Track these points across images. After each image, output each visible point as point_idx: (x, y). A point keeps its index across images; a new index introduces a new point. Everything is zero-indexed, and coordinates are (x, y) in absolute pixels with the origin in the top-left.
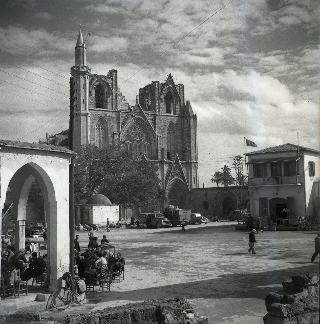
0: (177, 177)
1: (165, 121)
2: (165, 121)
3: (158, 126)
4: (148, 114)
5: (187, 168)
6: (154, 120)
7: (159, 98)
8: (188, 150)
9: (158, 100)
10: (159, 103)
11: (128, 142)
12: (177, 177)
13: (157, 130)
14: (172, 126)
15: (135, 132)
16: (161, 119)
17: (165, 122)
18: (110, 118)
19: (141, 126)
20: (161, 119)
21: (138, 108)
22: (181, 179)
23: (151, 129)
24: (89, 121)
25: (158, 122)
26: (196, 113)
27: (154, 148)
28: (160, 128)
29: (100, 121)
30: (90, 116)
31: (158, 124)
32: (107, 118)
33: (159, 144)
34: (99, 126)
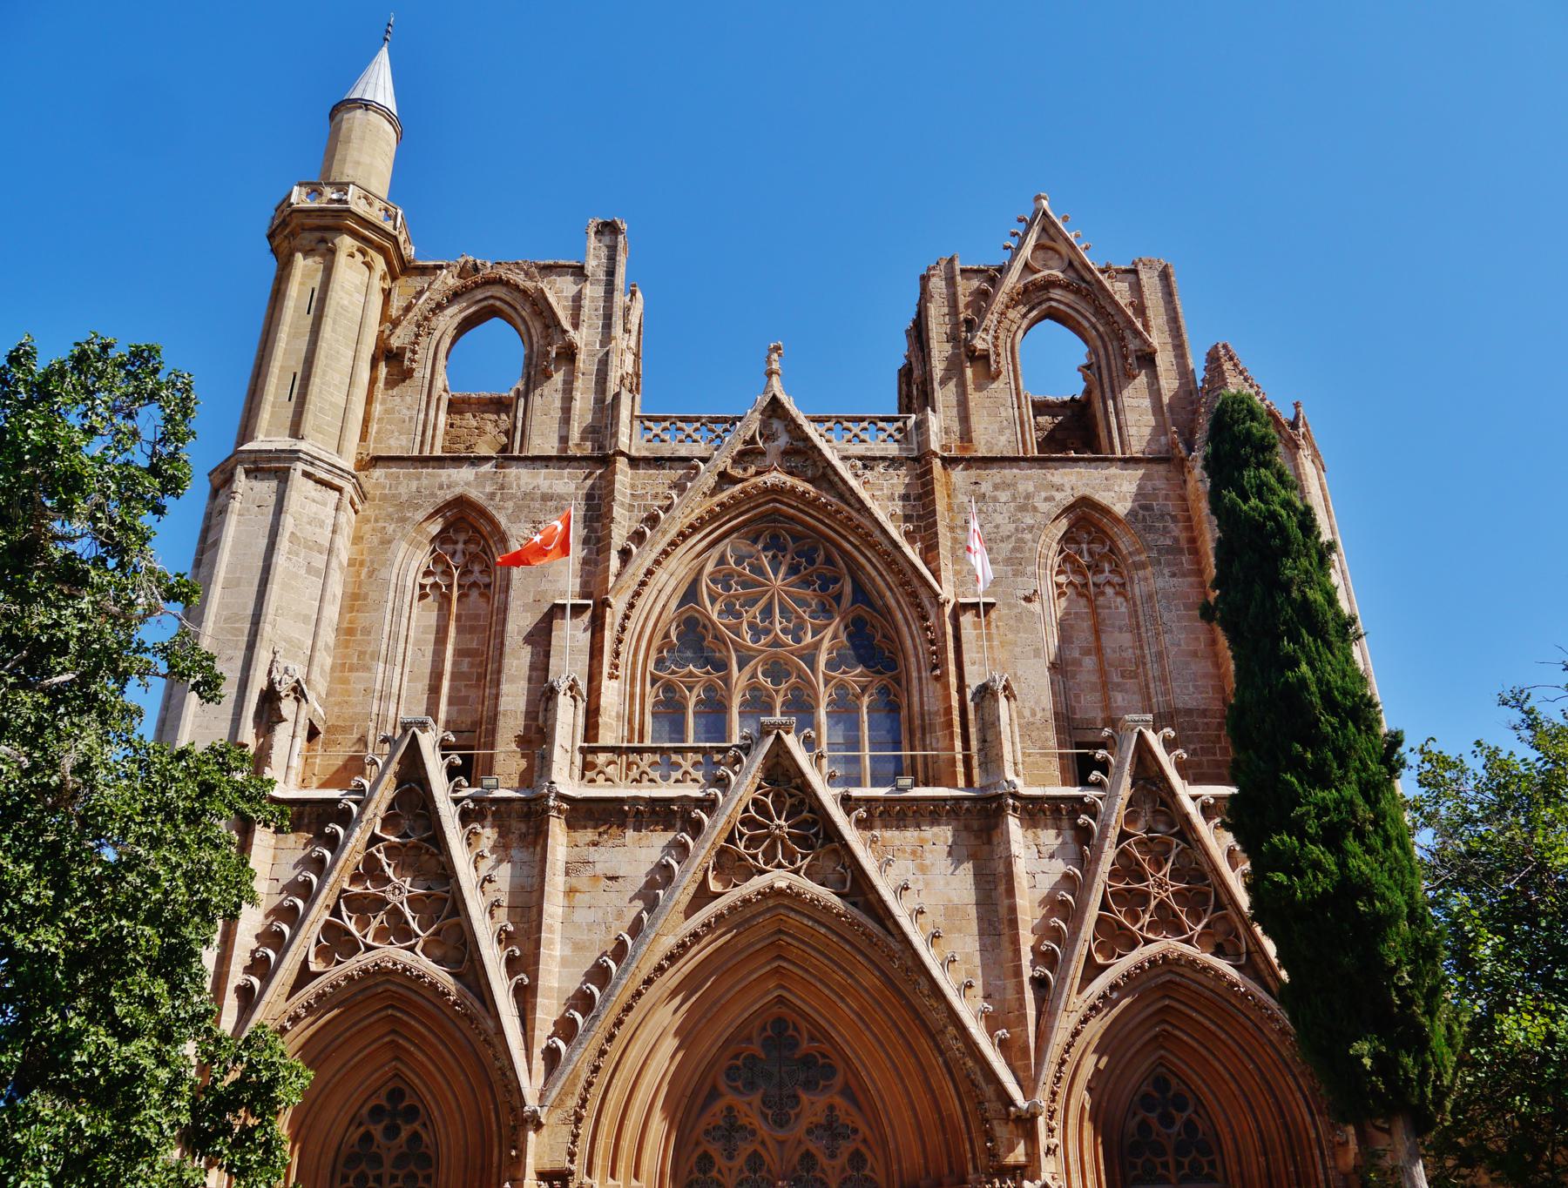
1: (1028, 496)
4: (868, 462)
6: (919, 497)
9: (954, 369)
10: (962, 385)
11: (691, 674)
14: (1101, 535)
16: (986, 487)
17: (1022, 508)
19: (816, 550)
20: (986, 487)
21: (777, 425)
22: (1223, 965)
23: (891, 557)
25: (963, 509)
27: (933, 704)
29: (462, 537)
32: (510, 504)
33: (967, 668)
34: (447, 573)
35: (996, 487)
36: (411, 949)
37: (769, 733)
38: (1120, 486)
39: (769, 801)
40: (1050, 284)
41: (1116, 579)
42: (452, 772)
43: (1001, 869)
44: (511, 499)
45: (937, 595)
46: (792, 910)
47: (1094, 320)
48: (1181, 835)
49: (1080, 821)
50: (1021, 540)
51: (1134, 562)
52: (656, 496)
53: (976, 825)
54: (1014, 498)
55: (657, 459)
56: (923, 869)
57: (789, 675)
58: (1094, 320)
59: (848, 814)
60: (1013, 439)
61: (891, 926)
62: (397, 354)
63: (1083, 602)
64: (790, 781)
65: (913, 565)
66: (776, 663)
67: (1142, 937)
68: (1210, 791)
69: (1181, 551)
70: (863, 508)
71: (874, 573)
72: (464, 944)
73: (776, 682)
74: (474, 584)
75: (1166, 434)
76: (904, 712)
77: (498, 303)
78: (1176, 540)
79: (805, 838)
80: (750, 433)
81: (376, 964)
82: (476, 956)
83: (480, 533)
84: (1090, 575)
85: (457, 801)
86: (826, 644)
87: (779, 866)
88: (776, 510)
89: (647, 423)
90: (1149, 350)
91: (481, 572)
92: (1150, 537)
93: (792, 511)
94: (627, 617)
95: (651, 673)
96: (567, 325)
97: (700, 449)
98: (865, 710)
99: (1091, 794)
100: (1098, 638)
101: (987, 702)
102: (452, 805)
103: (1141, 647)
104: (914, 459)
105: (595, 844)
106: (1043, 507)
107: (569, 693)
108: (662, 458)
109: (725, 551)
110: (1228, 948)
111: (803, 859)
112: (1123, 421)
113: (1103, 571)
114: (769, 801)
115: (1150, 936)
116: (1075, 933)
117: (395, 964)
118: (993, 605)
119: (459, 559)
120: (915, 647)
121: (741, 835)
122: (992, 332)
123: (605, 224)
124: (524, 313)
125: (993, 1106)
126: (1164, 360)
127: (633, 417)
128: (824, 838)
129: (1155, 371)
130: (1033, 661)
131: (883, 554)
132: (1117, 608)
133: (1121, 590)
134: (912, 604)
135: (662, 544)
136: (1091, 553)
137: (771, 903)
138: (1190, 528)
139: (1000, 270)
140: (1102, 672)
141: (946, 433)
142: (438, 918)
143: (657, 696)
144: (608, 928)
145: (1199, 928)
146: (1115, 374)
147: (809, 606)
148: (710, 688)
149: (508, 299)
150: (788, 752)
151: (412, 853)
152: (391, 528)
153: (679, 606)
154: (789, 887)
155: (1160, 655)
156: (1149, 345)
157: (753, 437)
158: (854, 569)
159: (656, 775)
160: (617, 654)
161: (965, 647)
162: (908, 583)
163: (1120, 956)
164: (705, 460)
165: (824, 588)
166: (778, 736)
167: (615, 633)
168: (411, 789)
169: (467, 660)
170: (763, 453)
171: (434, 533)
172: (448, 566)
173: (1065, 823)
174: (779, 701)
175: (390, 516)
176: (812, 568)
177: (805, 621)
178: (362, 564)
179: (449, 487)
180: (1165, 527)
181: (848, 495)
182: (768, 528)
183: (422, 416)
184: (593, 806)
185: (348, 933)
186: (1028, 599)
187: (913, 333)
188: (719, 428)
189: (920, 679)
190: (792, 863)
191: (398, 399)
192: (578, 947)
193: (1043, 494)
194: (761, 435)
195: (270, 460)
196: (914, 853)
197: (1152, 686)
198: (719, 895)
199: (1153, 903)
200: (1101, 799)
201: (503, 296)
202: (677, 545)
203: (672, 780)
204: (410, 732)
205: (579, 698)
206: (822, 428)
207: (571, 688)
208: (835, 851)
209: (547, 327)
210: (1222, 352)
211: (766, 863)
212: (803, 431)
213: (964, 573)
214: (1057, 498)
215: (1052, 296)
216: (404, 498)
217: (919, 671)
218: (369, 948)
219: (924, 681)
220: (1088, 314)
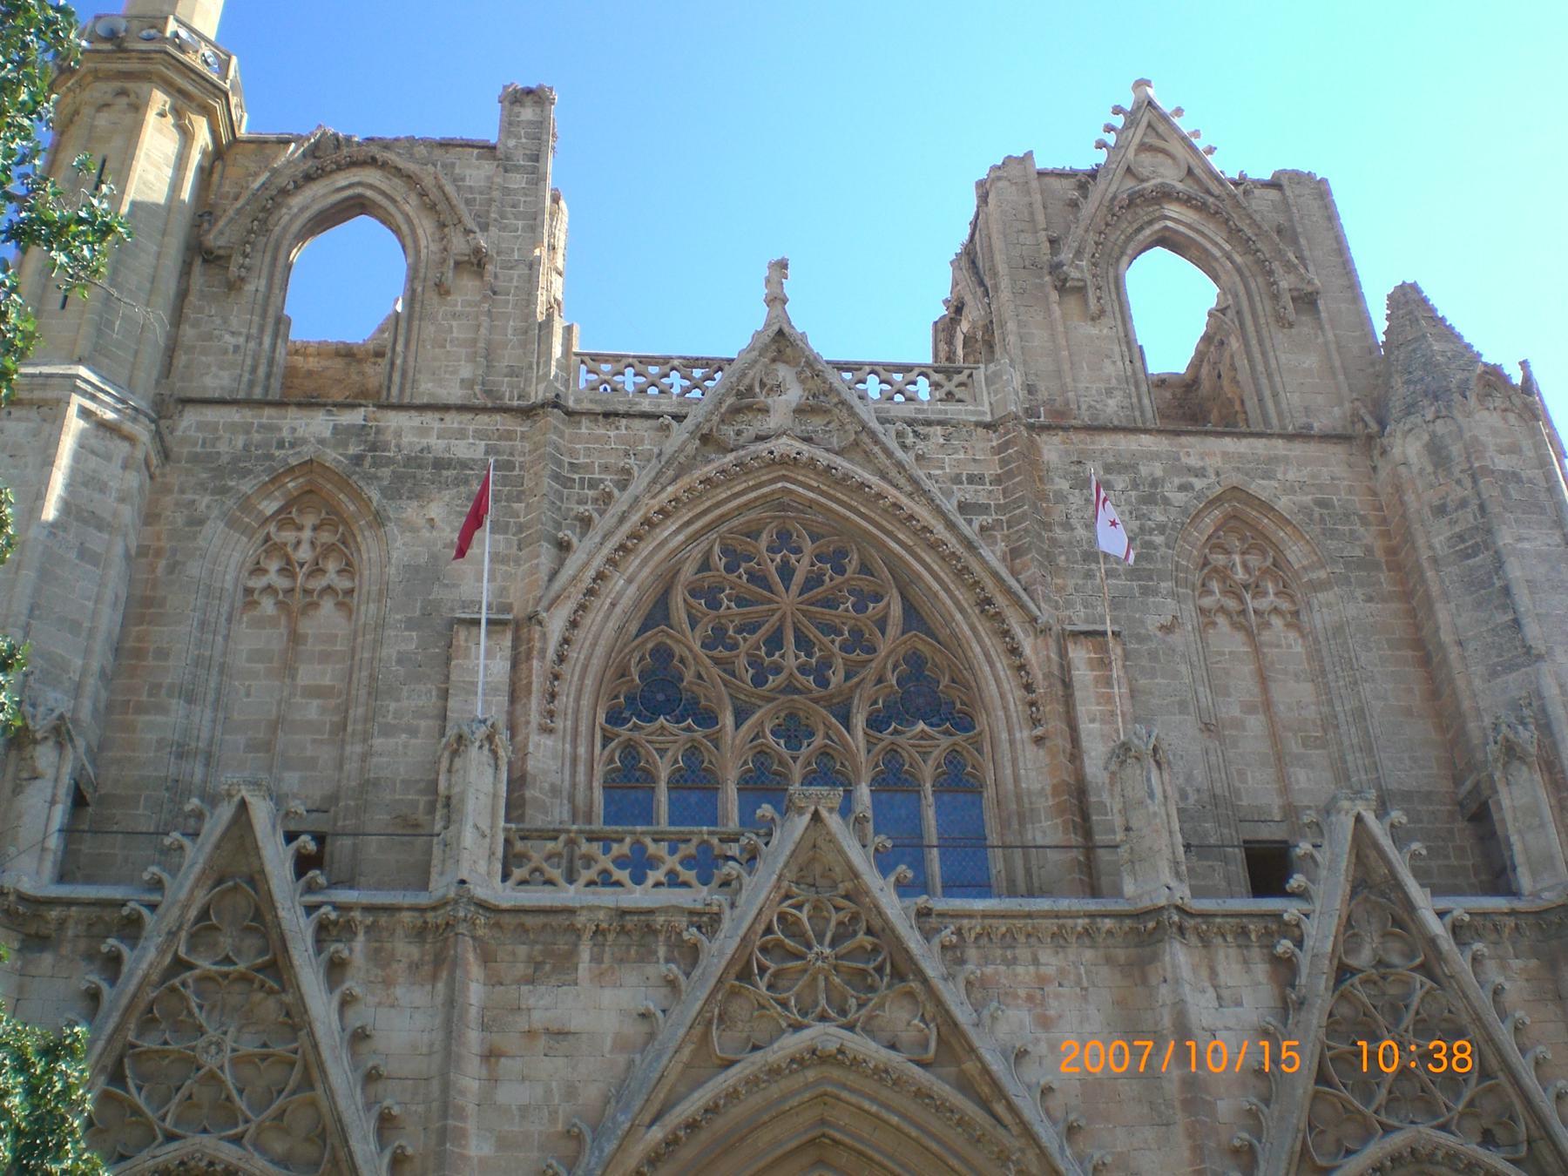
1: (1154, 483)
3: (1058, 532)
6: (998, 480)
8: (1511, 752)
14: (1259, 542)
17: (1149, 500)
18: (427, 473)
19: (842, 553)
21: (784, 372)
26: (1524, 365)
29: (309, 520)
32: (386, 472)
35: (1108, 469)
36: (237, 1140)
37: (801, 811)
38: (1285, 473)
39: (803, 916)
40: (1166, 194)
41: (1285, 605)
42: (304, 864)
43: (1167, 1021)
44: (387, 465)
45: (1035, 619)
46: (844, 1086)
48: (1424, 969)
49: (1280, 949)
50: (1149, 545)
51: (1310, 581)
53: (1121, 954)
54: (1135, 486)
55: (606, 415)
56: (1045, 1023)
57: (812, 734)
58: (1228, 247)
59: (927, 935)
61: (1000, 1108)
62: (219, 257)
63: (1240, 637)
64: (834, 886)
65: (995, 575)
66: (791, 716)
67: (1380, 1123)
68: (1461, 906)
69: (1376, 566)
70: (918, 490)
71: (936, 587)
72: (323, 1135)
73: (793, 740)
74: (329, 589)
75: (1341, 404)
76: (989, 793)
77: (369, 193)
78: (1369, 550)
79: (863, 973)
80: (747, 381)
81: (182, 1163)
82: (342, 1154)
83: (337, 514)
84: (1248, 597)
85: (310, 909)
86: (869, 689)
87: (823, 1018)
88: (784, 489)
90: (1309, 289)
91: (339, 572)
92: (1332, 544)
93: (811, 495)
94: (566, 641)
95: (603, 729)
96: (471, 224)
98: (928, 787)
100: (1265, 690)
101: (1129, 771)
102: (300, 911)
103: (1330, 703)
104: (987, 426)
105: (531, 981)
106: (1179, 498)
107: (487, 746)
108: (617, 415)
109: (712, 547)
110: (1500, 1134)
111: (860, 1006)
112: (1279, 386)
113: (1265, 594)
114: (803, 916)
117: (211, 1164)
119: (304, 554)
120: (1002, 696)
121: (763, 970)
122: (1087, 256)
123: (529, 92)
124: (407, 208)
128: (892, 976)
129: (1319, 319)
130: (1178, 718)
131: (948, 558)
132: (1290, 646)
133: (1294, 620)
134: (995, 633)
136: (1245, 566)
137: (811, 1075)
138: (1386, 534)
139: (1093, 174)
140: (1274, 737)
141: (1030, 392)
142: (280, 1092)
143: (611, 761)
144: (553, 1114)
145: (1460, 1107)
146: (1262, 321)
148: (693, 751)
149: (384, 187)
150: (832, 840)
151: (237, 988)
152: (204, 501)
153: (643, 629)
154: (840, 1051)
155: (1360, 714)
156: (1310, 282)
157: (750, 389)
158: (905, 584)
159: (623, 875)
160: (553, 696)
161: (1078, 694)
162: (989, 601)
163: (1349, 1153)
164: (679, 418)
165: (860, 607)
166: (816, 817)
167: (548, 663)
168: (236, 888)
169: (315, 703)
170: (765, 411)
171: (269, 512)
172: (289, 561)
173: (1256, 953)
174: (797, 771)
175: (202, 487)
176: (839, 579)
177: (833, 654)
178: (158, 553)
179: (292, 445)
180: (1352, 532)
181: (893, 473)
182: (774, 518)
183: (252, 345)
184: (529, 921)
185: (137, 1111)
186: (1167, 629)
187: (964, 263)
188: (697, 373)
189: (1012, 742)
190: (843, 1012)
191: (218, 321)
192: (503, 1143)
193: (1177, 481)
194: (762, 385)
196: (1030, 998)
197: (1350, 758)
198: (731, 1064)
200: (1307, 916)
201: (377, 183)
202: (640, 538)
203: (650, 881)
204: (236, 799)
205: (501, 753)
206: (847, 376)
207: (490, 738)
208: (911, 995)
209: (442, 225)
211: (804, 1014)
213: (1070, 590)
215: (1167, 213)
216: (225, 459)
217: (1010, 731)
218: (171, 1137)
219: (1019, 746)
220: (1221, 242)
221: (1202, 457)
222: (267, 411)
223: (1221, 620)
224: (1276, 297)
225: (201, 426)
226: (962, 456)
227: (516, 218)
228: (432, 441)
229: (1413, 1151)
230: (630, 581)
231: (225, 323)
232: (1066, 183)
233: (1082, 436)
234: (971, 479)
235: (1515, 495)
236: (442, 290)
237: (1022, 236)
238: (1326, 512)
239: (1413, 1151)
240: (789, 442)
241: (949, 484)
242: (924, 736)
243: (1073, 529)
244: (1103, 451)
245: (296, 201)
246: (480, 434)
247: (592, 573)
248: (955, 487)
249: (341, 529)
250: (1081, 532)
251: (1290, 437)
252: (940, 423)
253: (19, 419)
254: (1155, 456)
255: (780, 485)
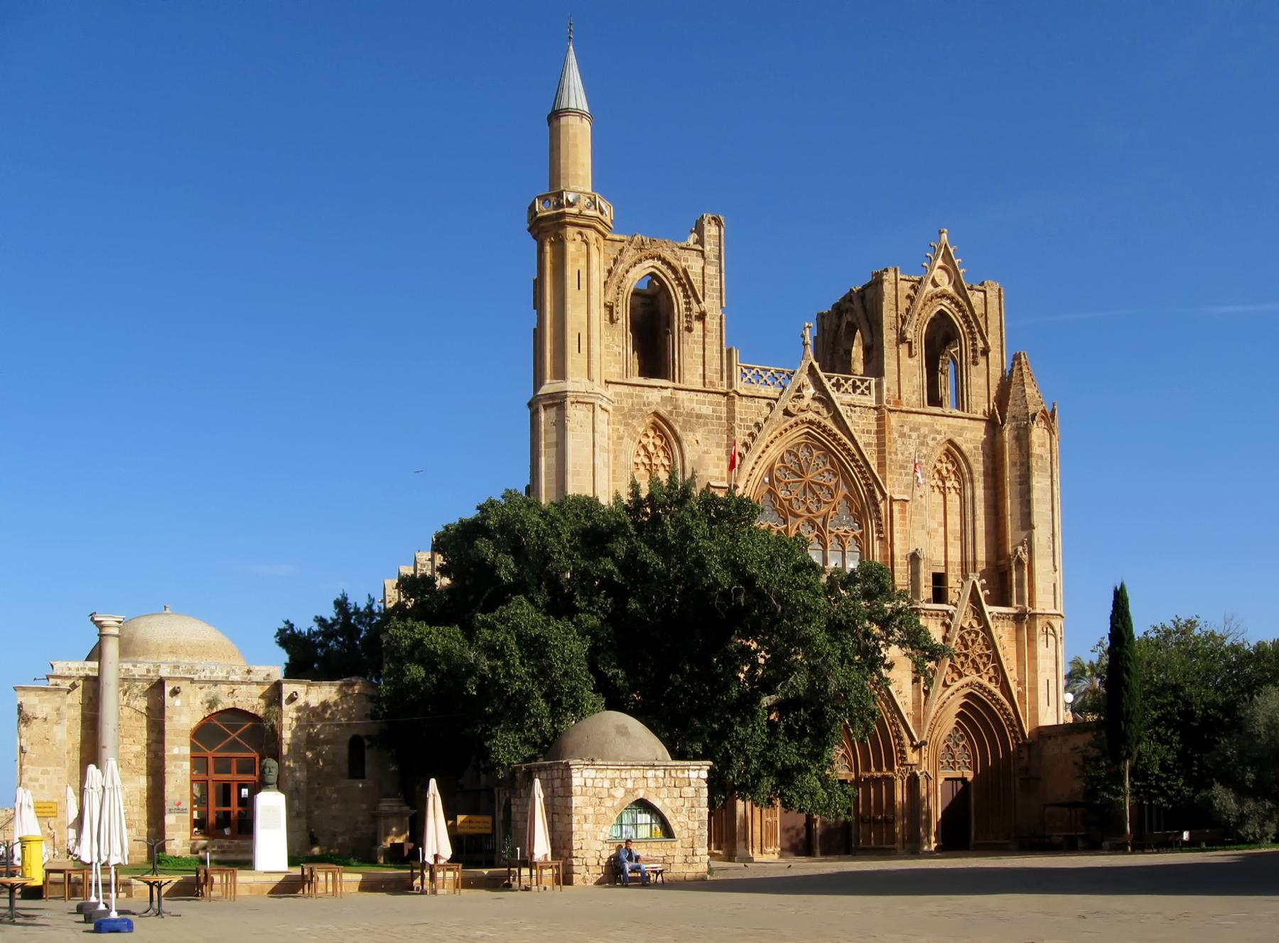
0: (973, 677)
1: (925, 436)
2: (925, 436)
3: (893, 456)
5: (1018, 641)
7: (902, 339)
12: (973, 677)
13: (888, 476)
15: (801, 481)
16: (906, 429)
17: (922, 444)
20: (906, 429)
21: (807, 381)
24: (602, 427)
25: (895, 442)
28: (902, 467)
30: (604, 405)
31: (894, 450)
32: (680, 419)
33: (896, 535)
40: (943, 295)
47: (961, 322)
52: (751, 420)
54: (919, 437)
55: (751, 397)
58: (961, 322)
60: (919, 398)
63: (942, 496)
68: (997, 609)
77: (657, 272)
89: (745, 371)
97: (772, 391)
99: (951, 609)
104: (875, 408)
106: (931, 443)
115: (966, 673)
116: (942, 671)
118: (907, 501)
122: (914, 327)
125: (907, 741)
126: (994, 354)
127: (737, 365)
132: (955, 501)
135: (759, 453)
136: (947, 468)
147: (822, 490)
149: (663, 270)
152: (622, 428)
164: (777, 400)
170: (803, 397)
172: (648, 452)
175: (620, 422)
179: (648, 405)
186: (921, 496)
193: (932, 436)
195: (584, 397)
199: (970, 659)
209: (686, 296)
210: (1023, 357)
212: (825, 387)
214: (938, 439)
216: (626, 410)
221: (941, 425)
222: (637, 388)
223: (936, 490)
224: (974, 351)
225: (616, 394)
226: (865, 421)
227: (713, 292)
228: (695, 405)
229: (971, 683)
230: (760, 469)
231: (613, 339)
232: (910, 284)
233: (904, 414)
234: (867, 433)
235: (1039, 465)
236: (689, 329)
237: (892, 312)
238: (976, 452)
239: (971, 683)
240: (812, 414)
241: (860, 434)
242: (846, 531)
243: (897, 455)
244: (910, 422)
245: (630, 275)
246: (711, 403)
247: (751, 468)
248: (862, 435)
249: (664, 439)
250: (900, 455)
251: (970, 419)
252: (860, 406)
253: (579, 410)
254: (926, 425)
255: (807, 430)
